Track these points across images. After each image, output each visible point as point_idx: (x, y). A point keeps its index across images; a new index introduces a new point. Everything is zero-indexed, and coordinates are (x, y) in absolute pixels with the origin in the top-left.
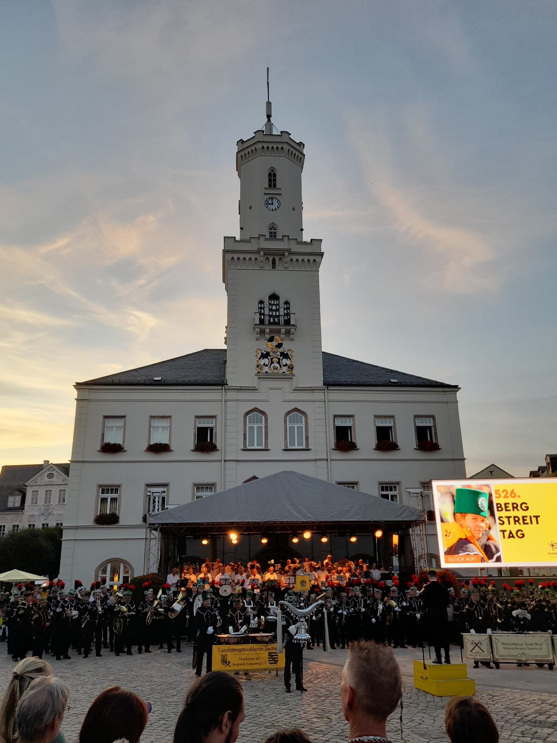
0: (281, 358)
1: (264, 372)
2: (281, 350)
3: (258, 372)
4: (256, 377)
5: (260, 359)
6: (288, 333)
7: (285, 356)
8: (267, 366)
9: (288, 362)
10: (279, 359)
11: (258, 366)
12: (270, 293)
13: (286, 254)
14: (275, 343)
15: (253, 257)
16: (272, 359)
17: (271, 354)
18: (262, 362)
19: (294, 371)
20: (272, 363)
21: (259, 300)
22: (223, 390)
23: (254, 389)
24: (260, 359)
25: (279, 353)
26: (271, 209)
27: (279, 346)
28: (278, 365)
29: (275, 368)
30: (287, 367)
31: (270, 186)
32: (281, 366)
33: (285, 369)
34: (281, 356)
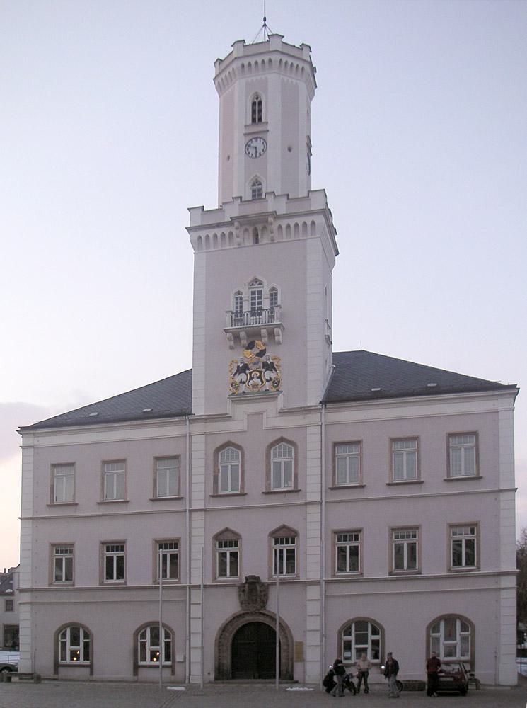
0: (263, 370)
1: (240, 391)
2: (263, 359)
3: (233, 394)
4: (229, 401)
6: (271, 334)
7: (270, 367)
8: (244, 383)
9: (273, 375)
10: (260, 372)
13: (271, 219)
14: (256, 351)
16: (251, 373)
17: (250, 366)
19: (281, 388)
20: (251, 378)
22: (188, 422)
27: (261, 353)
29: (255, 386)
31: (254, 120)
32: (262, 382)
34: (263, 368)
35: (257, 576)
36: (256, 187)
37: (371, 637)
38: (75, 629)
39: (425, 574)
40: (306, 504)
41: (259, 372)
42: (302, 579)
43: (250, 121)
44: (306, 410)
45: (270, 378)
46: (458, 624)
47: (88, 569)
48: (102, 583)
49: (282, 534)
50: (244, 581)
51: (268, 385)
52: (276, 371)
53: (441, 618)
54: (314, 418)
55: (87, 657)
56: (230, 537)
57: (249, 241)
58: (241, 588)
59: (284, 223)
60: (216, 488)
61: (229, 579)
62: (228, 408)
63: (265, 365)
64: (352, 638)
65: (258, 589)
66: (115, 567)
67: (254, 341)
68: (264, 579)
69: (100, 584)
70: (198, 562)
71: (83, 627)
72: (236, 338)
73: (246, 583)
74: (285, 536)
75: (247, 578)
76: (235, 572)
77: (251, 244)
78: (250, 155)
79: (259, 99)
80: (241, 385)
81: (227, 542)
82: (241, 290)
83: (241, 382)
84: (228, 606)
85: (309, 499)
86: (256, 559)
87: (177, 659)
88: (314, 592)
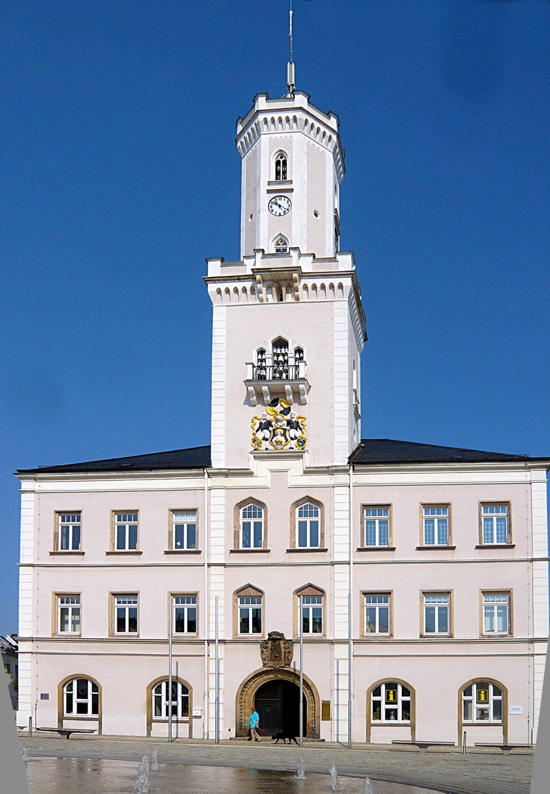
0: (288, 428)
2: (288, 417)
4: (252, 456)
5: (257, 431)
6: (297, 394)
8: (267, 440)
9: (298, 433)
10: (285, 430)
11: (254, 441)
12: (275, 336)
15: (248, 285)
17: (273, 423)
18: (260, 435)
20: (275, 435)
21: (258, 347)
22: (206, 474)
23: (247, 473)
24: (257, 431)
25: (286, 423)
26: (278, 214)
27: (286, 411)
28: (282, 439)
30: (296, 441)
32: (287, 440)
33: (293, 443)
35: (280, 632)
37: (401, 698)
38: (83, 682)
39: (456, 637)
40: (333, 564)
41: (283, 429)
42: (329, 637)
43: (273, 178)
44: (331, 471)
45: (295, 436)
46: (491, 688)
47: (96, 619)
48: (111, 634)
49: (307, 591)
50: (267, 637)
51: (293, 443)
52: (301, 429)
53: (474, 681)
54: (342, 478)
55: (95, 710)
56: (252, 592)
57: (272, 298)
58: (264, 645)
59: (310, 282)
60: (236, 544)
61: (251, 635)
62: (254, 465)
63: (289, 423)
64: (382, 698)
65: (282, 645)
66: (127, 622)
67: (278, 399)
68: (288, 636)
69: (109, 636)
70: (218, 617)
71: (92, 680)
72: (260, 395)
73: (269, 639)
74: (312, 593)
75: (269, 635)
76: (257, 628)
77: (276, 301)
78: (274, 213)
79: (284, 159)
80: (264, 442)
81: (249, 594)
82: (265, 347)
83: (265, 439)
84: (250, 661)
85: (337, 558)
86: (282, 616)
87: (194, 714)
88: (341, 651)
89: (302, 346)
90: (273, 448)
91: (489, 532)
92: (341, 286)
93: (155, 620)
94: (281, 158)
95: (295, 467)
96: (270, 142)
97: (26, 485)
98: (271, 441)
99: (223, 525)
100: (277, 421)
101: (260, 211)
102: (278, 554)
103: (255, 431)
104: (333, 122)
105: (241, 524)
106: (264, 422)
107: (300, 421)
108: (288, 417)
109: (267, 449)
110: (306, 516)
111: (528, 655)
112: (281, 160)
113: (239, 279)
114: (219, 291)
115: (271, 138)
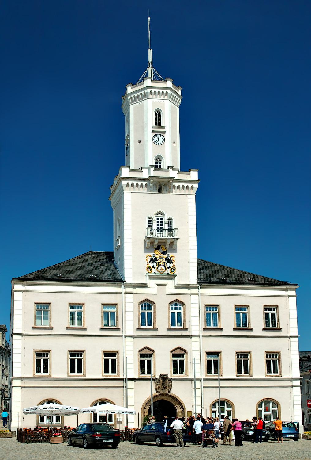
2: (166, 256)
5: (150, 262)
8: (155, 268)
10: (164, 263)
15: (144, 183)
17: (158, 259)
18: (151, 265)
20: (159, 266)
22: (123, 286)
23: (145, 286)
24: (150, 262)
25: (165, 259)
26: (157, 144)
28: (163, 268)
30: (170, 269)
32: (166, 268)
36: (158, 161)
52: (173, 263)
56: (148, 351)
59: (176, 184)
79: (159, 113)
80: (153, 269)
82: (152, 216)
89: (172, 217)
90: (158, 273)
91: (267, 321)
92: (192, 187)
93: (94, 366)
94: (158, 112)
95: (170, 284)
96: (152, 103)
97: (16, 287)
98: (158, 268)
99: (132, 314)
100: (161, 258)
101: (148, 141)
102: (162, 331)
103: (148, 263)
104: (180, 92)
105: (141, 313)
106: (153, 258)
107: (172, 258)
108: (166, 256)
109: (155, 273)
110: (175, 309)
111: (290, 387)
112: (158, 113)
113: (140, 179)
114: (128, 185)
115: (153, 101)
